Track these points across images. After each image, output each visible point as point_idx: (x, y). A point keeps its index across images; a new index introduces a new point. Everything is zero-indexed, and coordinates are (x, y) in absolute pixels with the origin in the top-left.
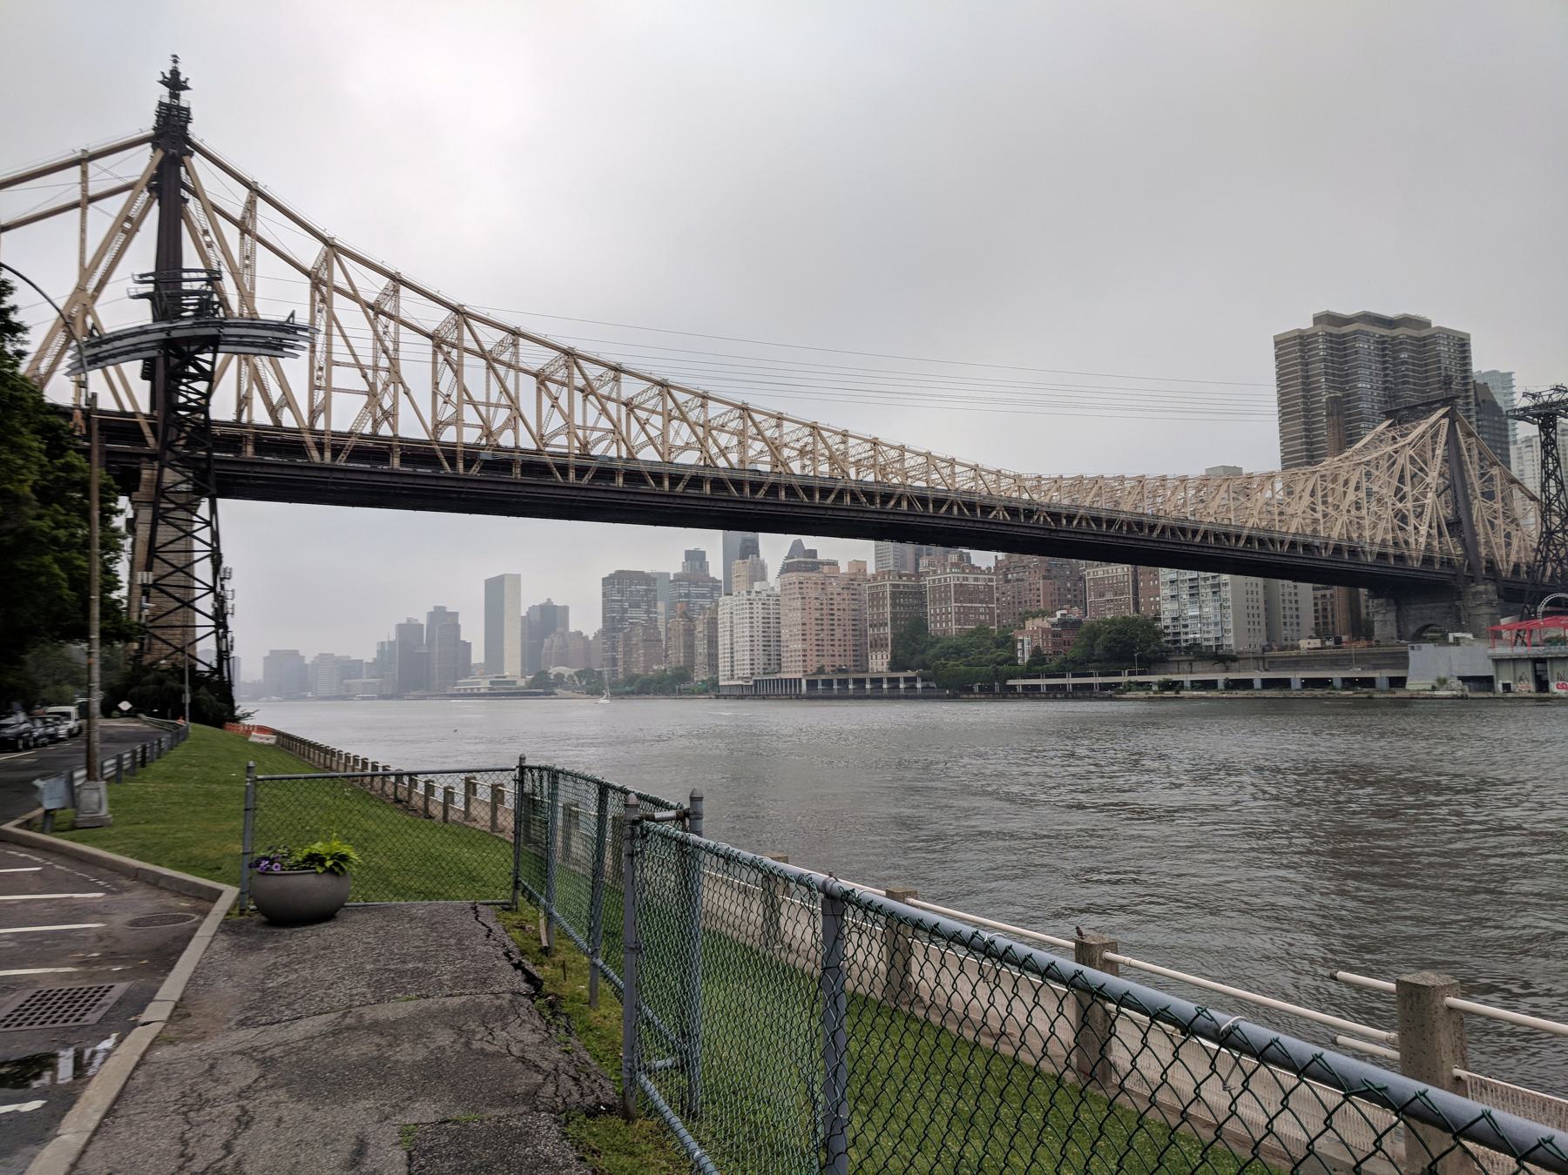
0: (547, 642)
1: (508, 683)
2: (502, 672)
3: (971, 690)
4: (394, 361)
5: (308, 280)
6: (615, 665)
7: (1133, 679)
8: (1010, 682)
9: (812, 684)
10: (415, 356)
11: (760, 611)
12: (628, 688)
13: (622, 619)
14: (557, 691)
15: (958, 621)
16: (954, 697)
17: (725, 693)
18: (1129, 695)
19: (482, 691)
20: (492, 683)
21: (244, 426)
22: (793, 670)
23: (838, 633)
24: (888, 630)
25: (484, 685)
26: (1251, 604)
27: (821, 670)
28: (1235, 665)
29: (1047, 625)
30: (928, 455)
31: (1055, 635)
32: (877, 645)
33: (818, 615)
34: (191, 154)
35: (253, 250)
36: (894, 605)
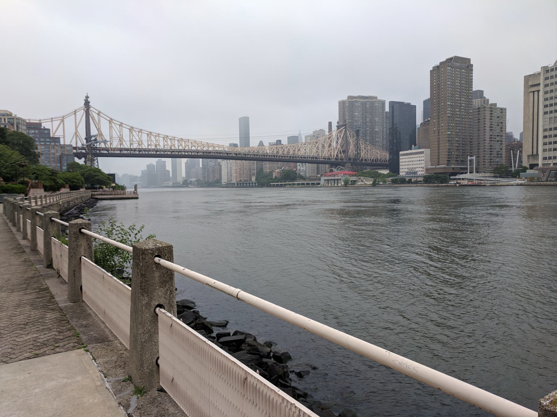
0: (192, 170)
1: (178, 183)
2: (177, 180)
3: (264, 185)
4: (122, 136)
5: (108, 122)
6: (205, 178)
7: (288, 183)
8: (271, 184)
9: (237, 184)
10: (126, 132)
11: (230, 165)
12: (205, 185)
13: (207, 165)
14: (189, 186)
15: (269, 169)
16: (262, 187)
17: (223, 186)
18: (287, 186)
19: (170, 186)
20: (173, 183)
21: (100, 148)
22: (234, 181)
23: (245, 172)
24: (255, 171)
25: (171, 184)
26: (313, 169)
27: (240, 181)
28: (306, 180)
29: (279, 171)
30: (218, 145)
31: (280, 173)
32: (254, 175)
33: (240, 167)
34: (90, 108)
35: (100, 118)
36: (257, 165)
